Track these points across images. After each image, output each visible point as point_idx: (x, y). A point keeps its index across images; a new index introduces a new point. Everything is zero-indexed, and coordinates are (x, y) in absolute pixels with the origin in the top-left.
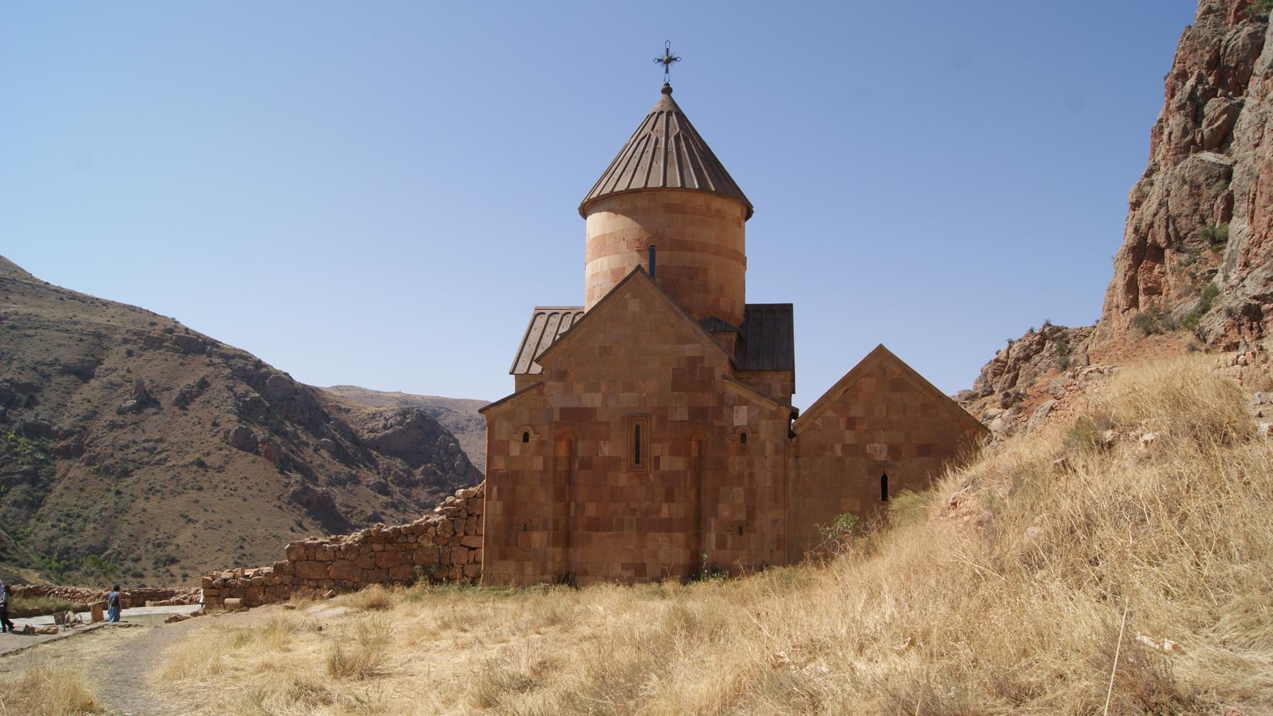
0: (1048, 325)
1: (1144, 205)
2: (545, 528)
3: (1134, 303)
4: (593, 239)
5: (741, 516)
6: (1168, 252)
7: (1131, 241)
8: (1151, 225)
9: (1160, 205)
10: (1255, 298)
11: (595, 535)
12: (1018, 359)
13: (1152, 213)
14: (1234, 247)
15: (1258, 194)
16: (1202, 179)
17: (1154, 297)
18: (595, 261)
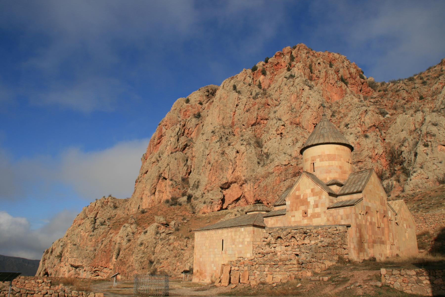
0: (110, 196)
1: (160, 164)
2: (367, 243)
3: (154, 193)
4: (328, 155)
5: (392, 241)
6: (168, 180)
7: (157, 174)
8: (164, 170)
9: (168, 165)
10: (212, 199)
11: (375, 245)
12: (99, 207)
13: (165, 166)
14: (196, 183)
15: (212, 169)
16: (181, 160)
17: (161, 194)
18: (331, 162)
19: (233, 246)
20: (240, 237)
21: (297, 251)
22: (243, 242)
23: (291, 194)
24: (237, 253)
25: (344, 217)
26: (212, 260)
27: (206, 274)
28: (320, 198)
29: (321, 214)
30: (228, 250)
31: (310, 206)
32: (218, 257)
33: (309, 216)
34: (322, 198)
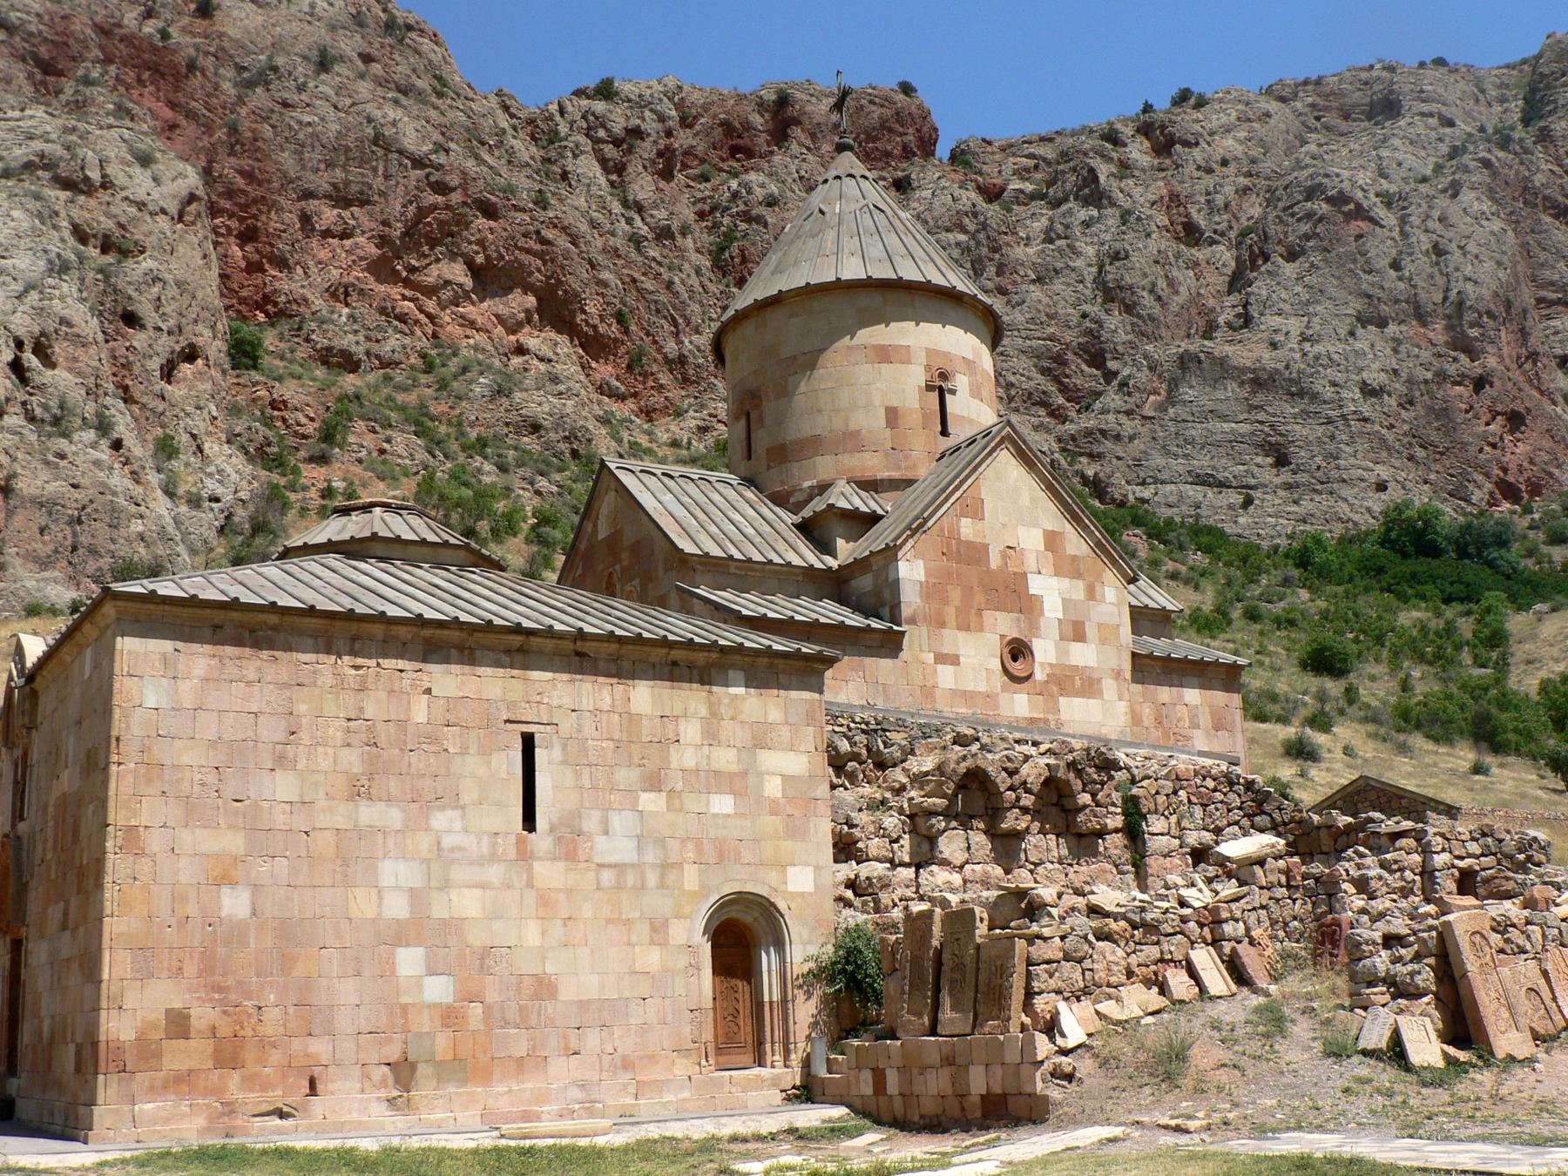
19: (651, 802)
20: (711, 736)
21: (1470, 856)
22: (745, 773)
23: (930, 524)
24: (691, 856)
25: (1205, 719)
26: (397, 908)
27: (320, 1047)
28: (1091, 593)
29: (1099, 680)
30: (591, 823)
31: (1042, 622)
32: (483, 886)
33: (1039, 675)
34: (1103, 600)
